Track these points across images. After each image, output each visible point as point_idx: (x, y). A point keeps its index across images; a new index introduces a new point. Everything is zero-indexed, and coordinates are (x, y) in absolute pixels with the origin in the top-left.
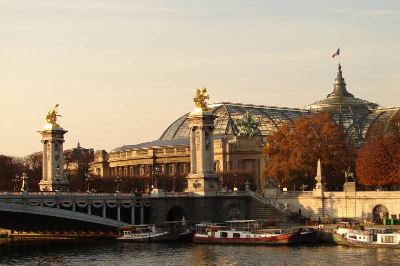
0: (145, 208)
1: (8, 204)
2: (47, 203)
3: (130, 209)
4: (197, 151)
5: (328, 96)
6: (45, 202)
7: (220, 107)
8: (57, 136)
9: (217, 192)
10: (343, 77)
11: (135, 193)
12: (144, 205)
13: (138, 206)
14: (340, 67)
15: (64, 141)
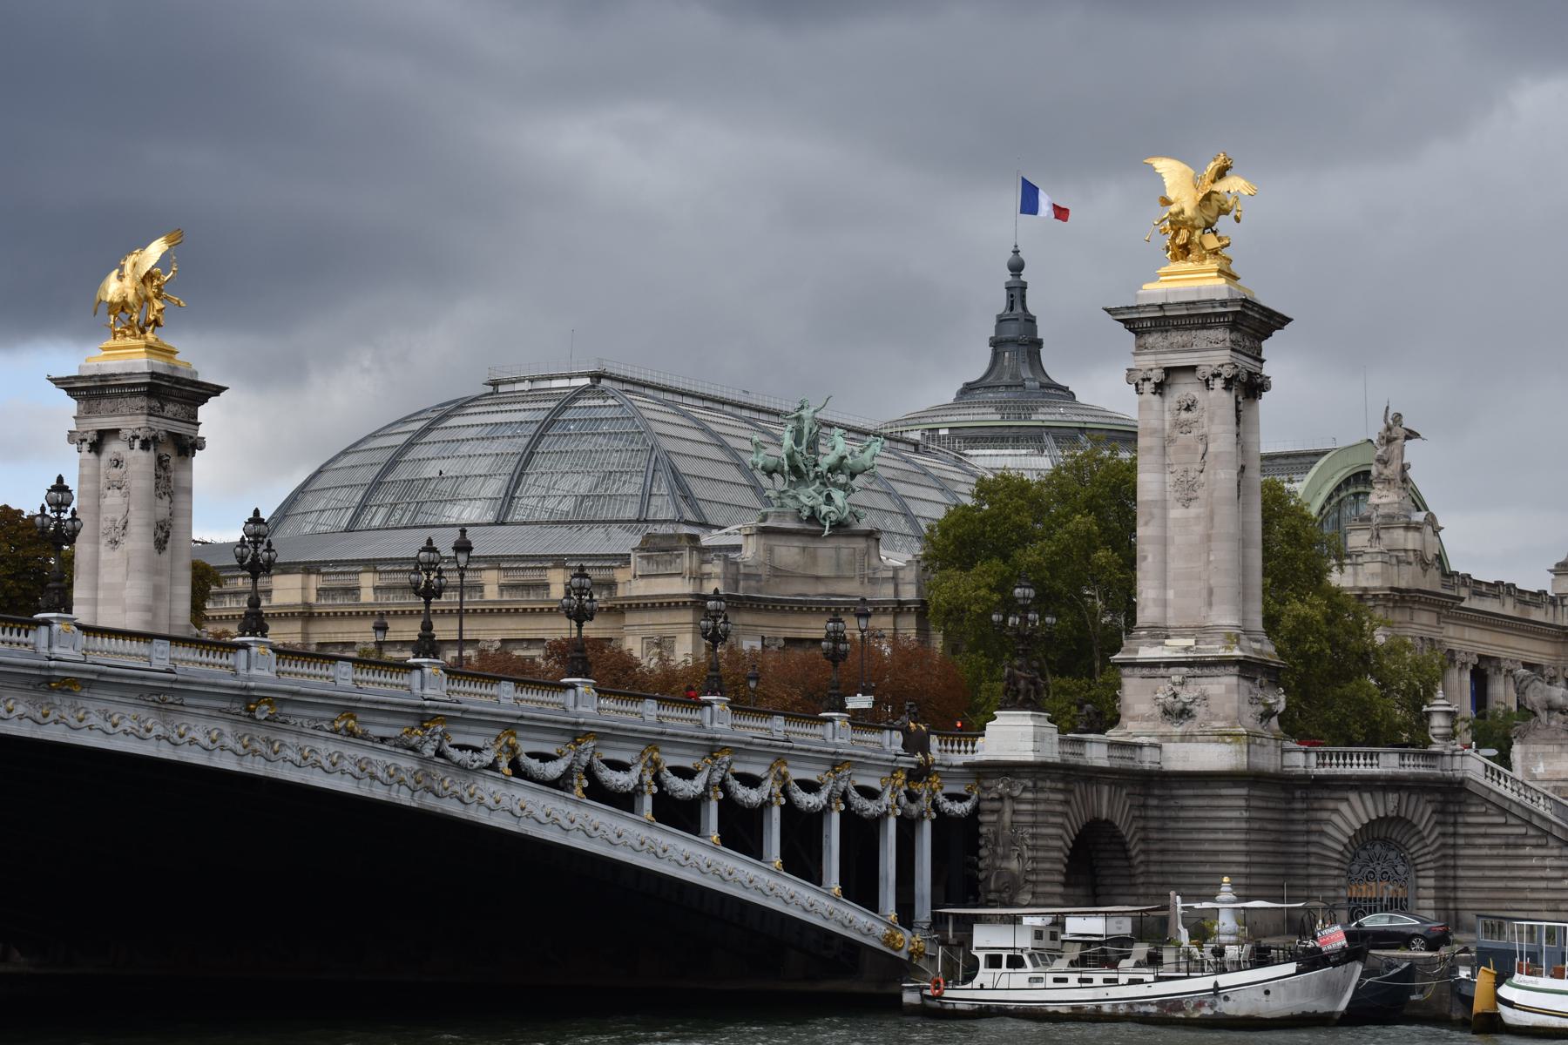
0: (943, 823)
1: (353, 752)
2: (532, 755)
3: (878, 821)
4: (1176, 513)
5: (968, 389)
6: (525, 747)
7: (581, 392)
8: (171, 408)
9: (1284, 751)
10: (1034, 303)
11: (906, 732)
12: (935, 805)
13: (914, 809)
14: (1017, 267)
15: (198, 444)
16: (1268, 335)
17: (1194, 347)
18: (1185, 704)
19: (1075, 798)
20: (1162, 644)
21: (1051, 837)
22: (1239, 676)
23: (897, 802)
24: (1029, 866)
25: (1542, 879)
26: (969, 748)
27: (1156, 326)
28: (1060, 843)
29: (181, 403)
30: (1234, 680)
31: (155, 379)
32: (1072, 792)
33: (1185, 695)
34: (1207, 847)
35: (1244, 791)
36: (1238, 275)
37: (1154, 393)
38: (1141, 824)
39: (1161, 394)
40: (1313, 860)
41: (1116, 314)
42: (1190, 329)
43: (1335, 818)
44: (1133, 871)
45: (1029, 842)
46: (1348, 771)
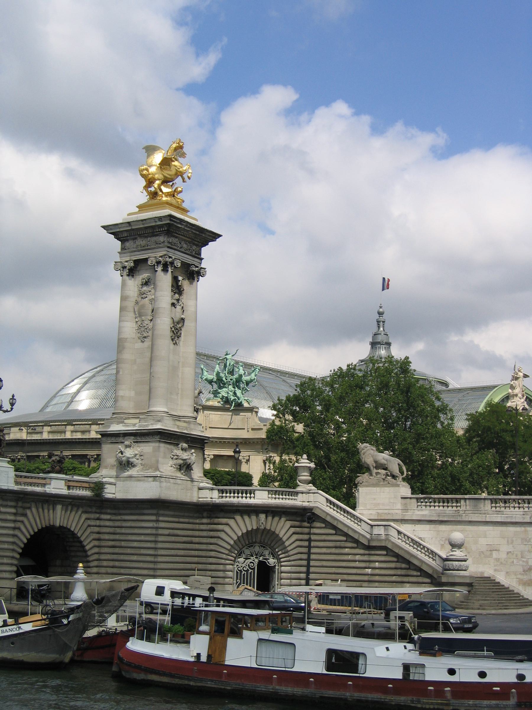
16: (205, 244)
17: (149, 247)
18: (129, 458)
20: (123, 422)
25: (354, 568)
27: (129, 236)
28: (11, 539)
30: (157, 444)
33: (129, 453)
34: (135, 544)
35: (154, 511)
36: (188, 209)
38: (96, 529)
40: (213, 554)
42: (147, 237)
43: (227, 529)
44: (88, 559)
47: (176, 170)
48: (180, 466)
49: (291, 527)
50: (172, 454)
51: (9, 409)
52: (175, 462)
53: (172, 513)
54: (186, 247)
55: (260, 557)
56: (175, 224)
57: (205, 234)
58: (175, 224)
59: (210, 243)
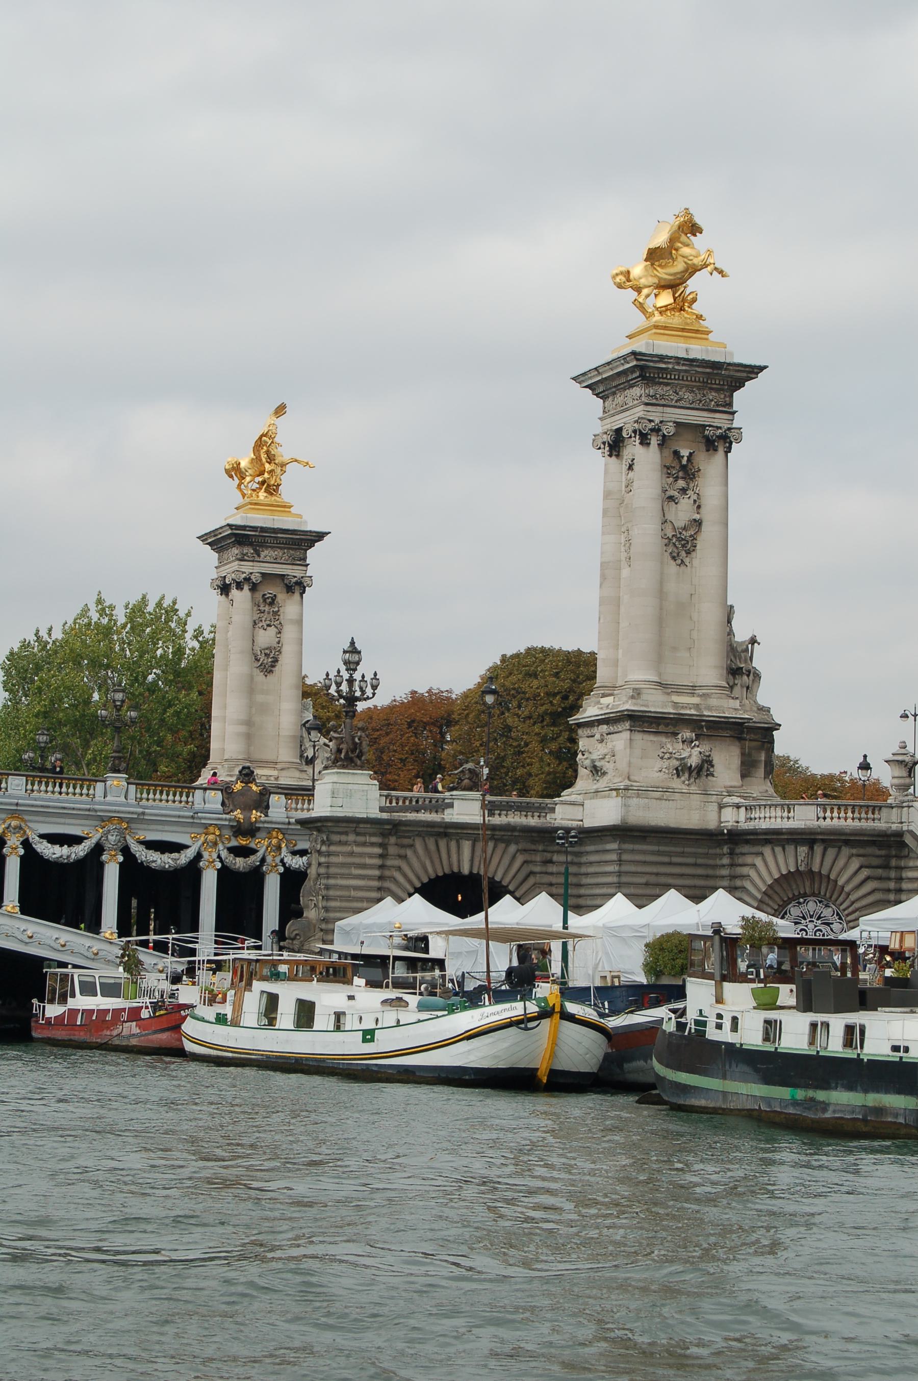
9: (721, 807)
12: (282, 861)
13: (240, 863)
16: (739, 384)
18: (593, 761)
19: (415, 852)
20: (599, 703)
21: (356, 888)
22: (631, 731)
23: (219, 857)
24: (323, 914)
26: (306, 806)
29: (281, 548)
30: (626, 735)
31: (236, 529)
32: (411, 846)
35: (614, 846)
37: (610, 456)
39: (618, 456)
41: (583, 381)
45: (324, 892)
46: (764, 825)
47: (685, 263)
48: (677, 769)
49: (861, 867)
50: (662, 750)
51: (371, 696)
52: (666, 763)
53: (656, 848)
54: (691, 398)
55: (818, 919)
56: (651, 364)
57: (726, 370)
58: (651, 364)
59: (746, 383)
